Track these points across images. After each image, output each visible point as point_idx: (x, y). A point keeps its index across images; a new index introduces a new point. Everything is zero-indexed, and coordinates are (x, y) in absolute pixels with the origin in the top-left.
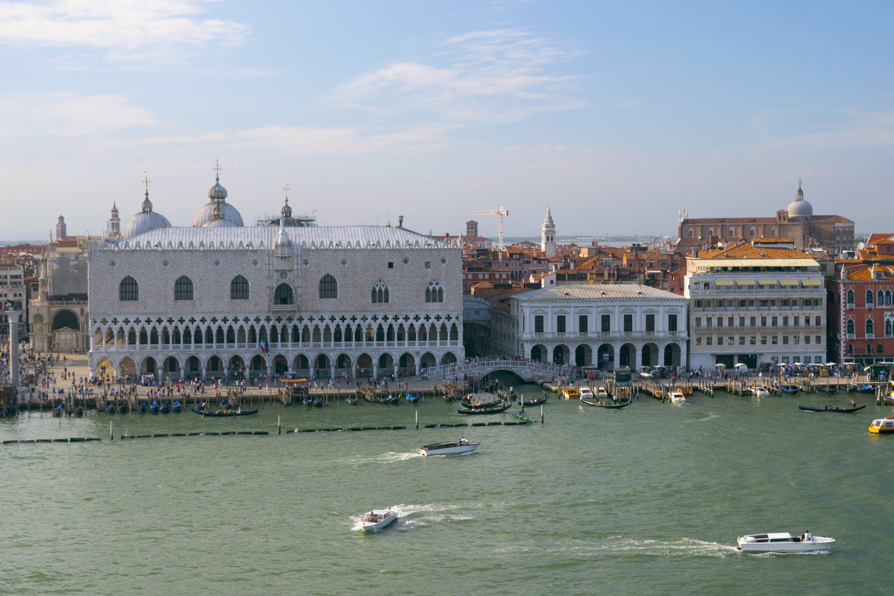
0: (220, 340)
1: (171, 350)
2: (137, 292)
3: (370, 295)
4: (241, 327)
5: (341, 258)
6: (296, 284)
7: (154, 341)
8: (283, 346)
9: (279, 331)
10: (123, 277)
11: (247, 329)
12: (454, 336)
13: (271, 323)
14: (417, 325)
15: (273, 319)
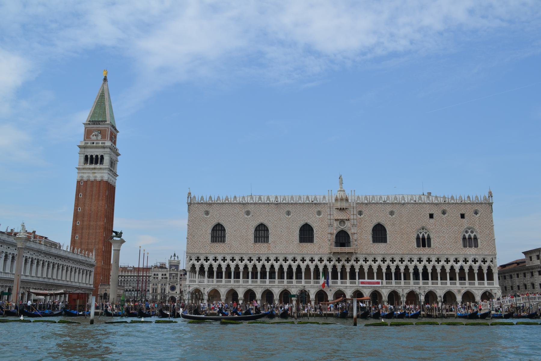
0: (290, 277)
1: (250, 284)
2: (224, 237)
3: (415, 241)
4: (308, 266)
5: (390, 210)
6: (353, 231)
7: (237, 276)
8: (342, 283)
9: (339, 270)
10: (214, 223)
11: (312, 268)
12: (490, 277)
13: (332, 263)
14: (457, 267)
15: (334, 260)
